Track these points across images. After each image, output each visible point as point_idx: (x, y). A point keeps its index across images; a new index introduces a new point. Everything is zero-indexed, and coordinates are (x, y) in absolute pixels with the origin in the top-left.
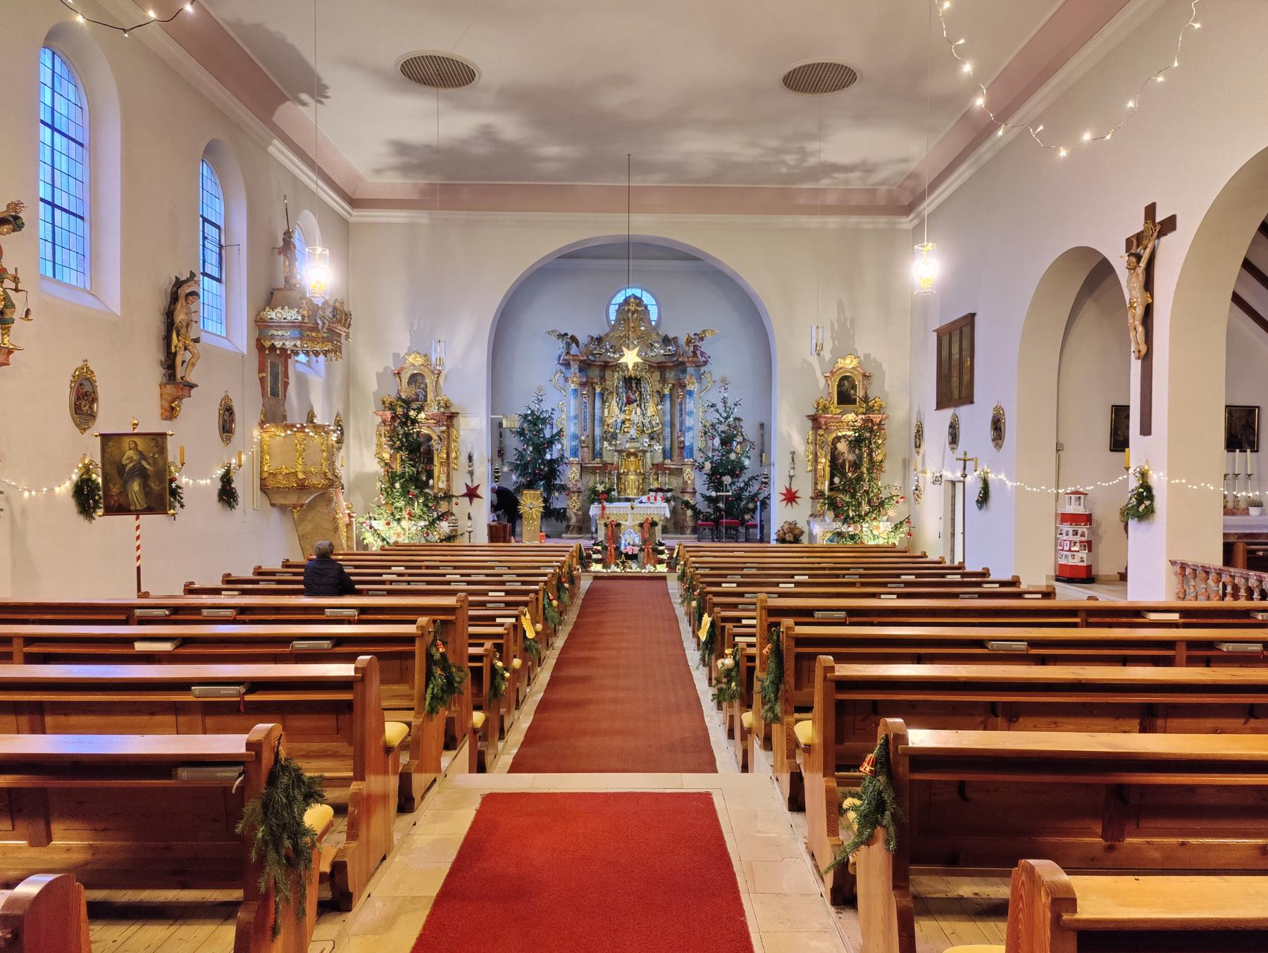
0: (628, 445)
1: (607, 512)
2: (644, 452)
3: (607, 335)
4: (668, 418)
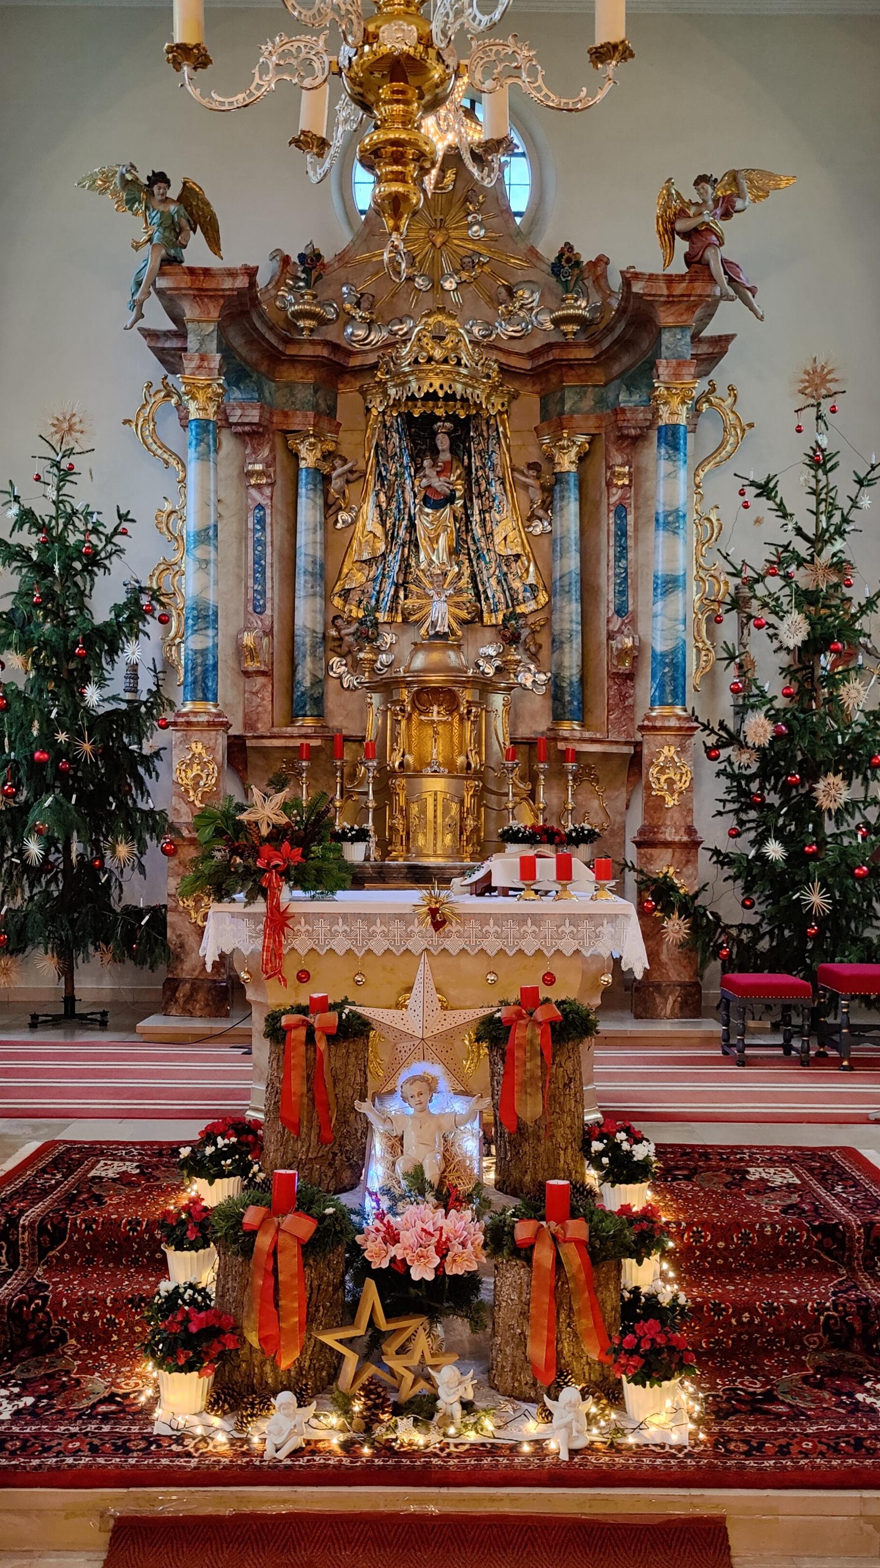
0: (420, 661)
1: (299, 942)
2: (485, 686)
3: (341, 257)
4: (572, 562)
